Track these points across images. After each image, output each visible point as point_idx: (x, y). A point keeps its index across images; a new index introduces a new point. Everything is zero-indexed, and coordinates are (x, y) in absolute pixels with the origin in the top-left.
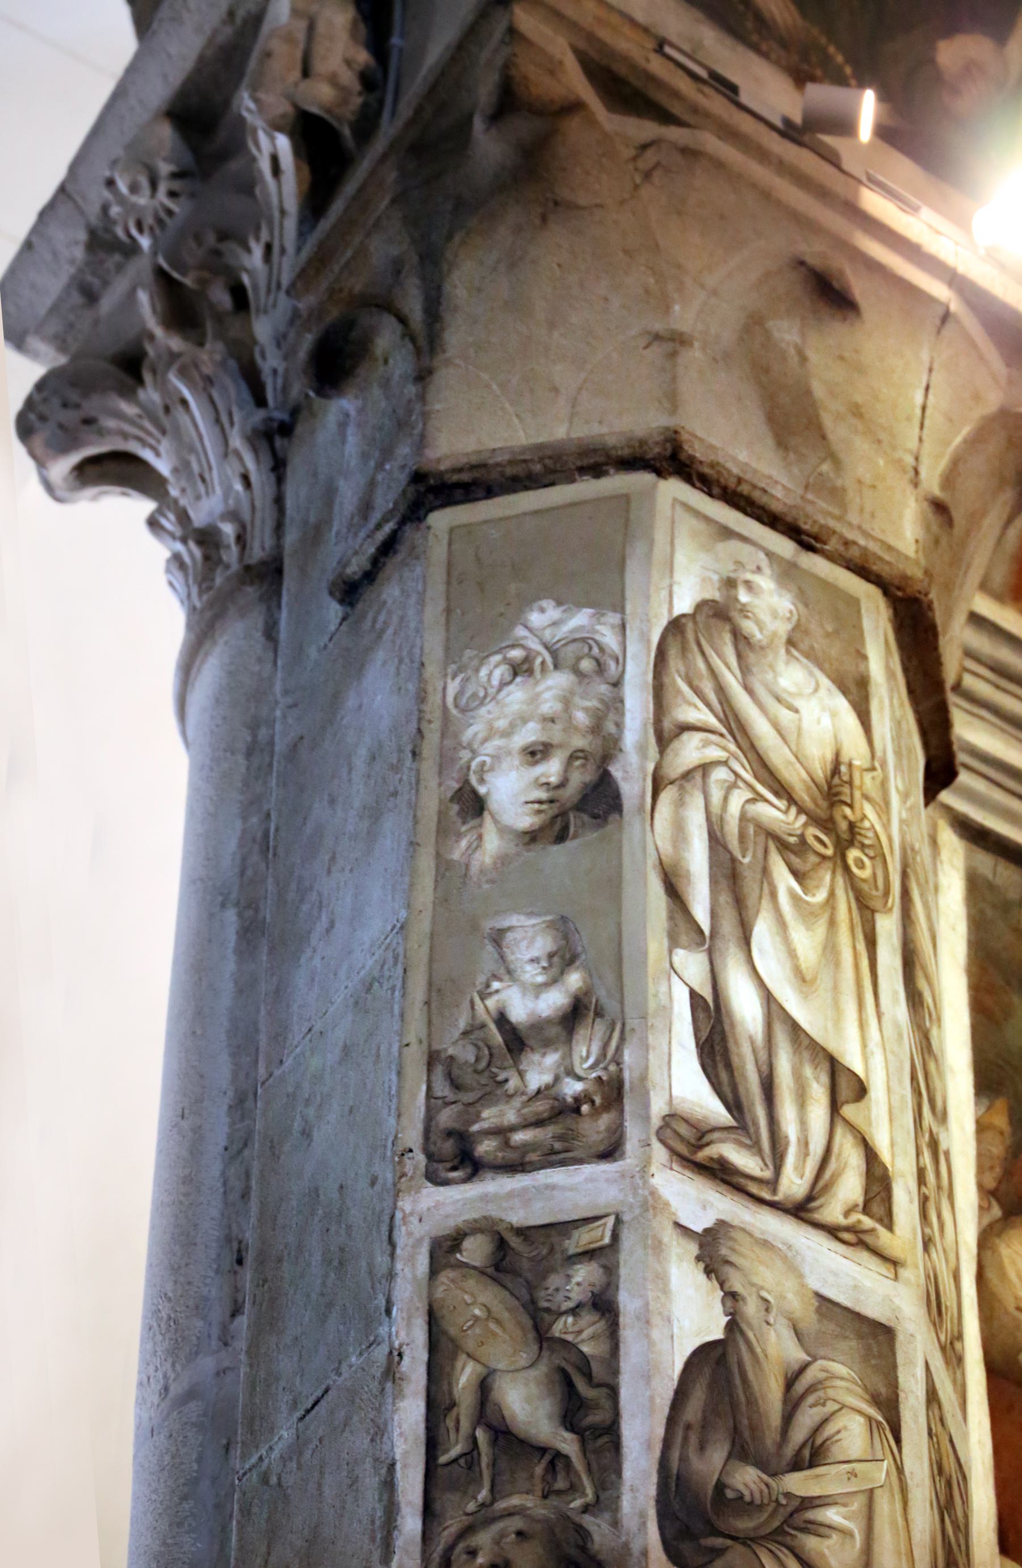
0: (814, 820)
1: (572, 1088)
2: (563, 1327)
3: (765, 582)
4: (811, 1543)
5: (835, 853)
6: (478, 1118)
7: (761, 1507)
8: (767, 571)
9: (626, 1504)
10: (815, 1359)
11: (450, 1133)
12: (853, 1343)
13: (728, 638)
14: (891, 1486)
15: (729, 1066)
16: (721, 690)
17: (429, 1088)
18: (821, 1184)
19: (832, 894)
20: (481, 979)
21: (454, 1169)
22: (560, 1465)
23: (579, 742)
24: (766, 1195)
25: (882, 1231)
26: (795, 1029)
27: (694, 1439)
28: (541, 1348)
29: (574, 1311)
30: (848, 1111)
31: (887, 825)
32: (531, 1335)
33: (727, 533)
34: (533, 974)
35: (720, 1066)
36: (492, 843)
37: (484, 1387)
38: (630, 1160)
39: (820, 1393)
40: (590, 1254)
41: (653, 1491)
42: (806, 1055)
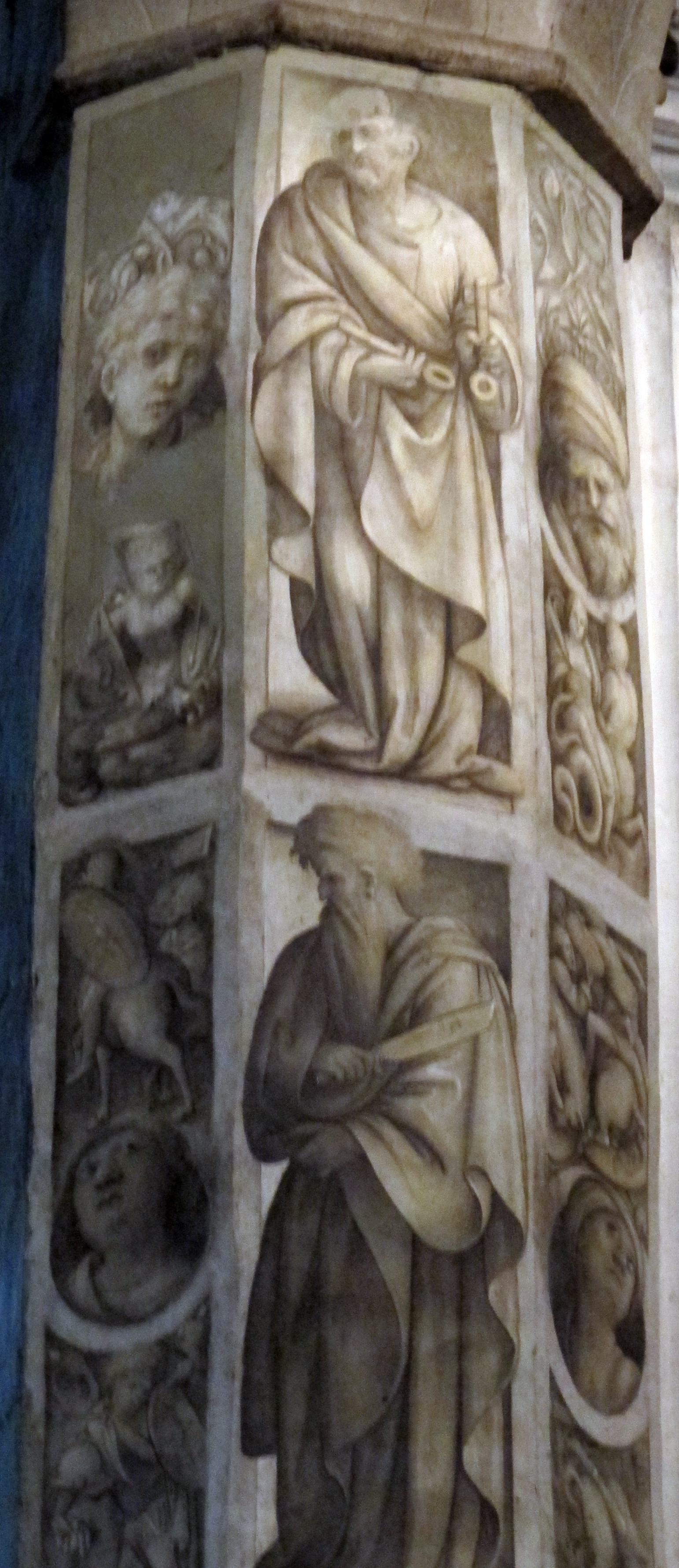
0: (435, 356)
1: (181, 698)
2: (169, 941)
3: (384, 123)
4: (408, 1106)
5: (457, 384)
6: (101, 737)
7: (357, 1081)
8: (385, 107)
9: (217, 1112)
10: (418, 919)
11: (78, 754)
12: (463, 891)
13: (341, 194)
14: (498, 1027)
15: (332, 645)
16: (332, 253)
17: (63, 708)
18: (432, 736)
19: (452, 429)
20: (107, 593)
21: (82, 789)
22: (165, 1079)
23: (192, 338)
24: (369, 765)
25: (499, 768)
26: (407, 582)
27: (284, 1037)
28: (150, 963)
29: (178, 924)
30: (465, 653)
31: (516, 337)
32: (142, 952)
33: (340, 84)
34: (149, 584)
35: (323, 646)
36: (119, 450)
37: (103, 1007)
38: (225, 770)
39: (425, 952)
40: (192, 866)
41: (239, 1095)
42: (419, 607)
